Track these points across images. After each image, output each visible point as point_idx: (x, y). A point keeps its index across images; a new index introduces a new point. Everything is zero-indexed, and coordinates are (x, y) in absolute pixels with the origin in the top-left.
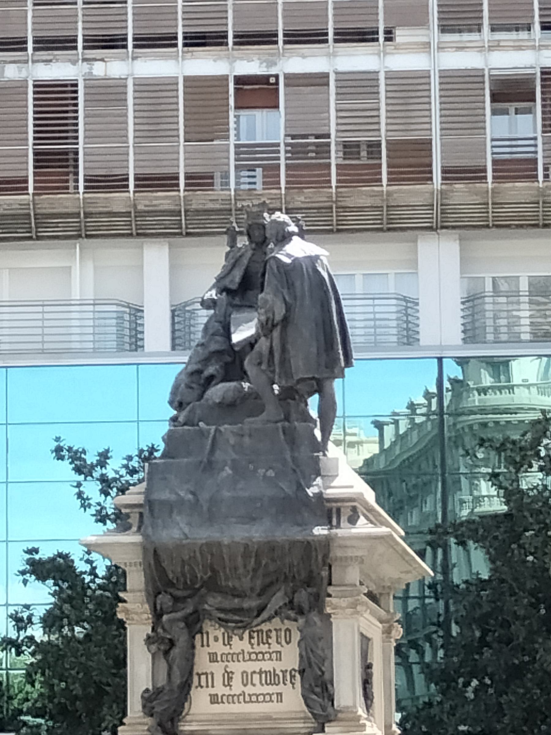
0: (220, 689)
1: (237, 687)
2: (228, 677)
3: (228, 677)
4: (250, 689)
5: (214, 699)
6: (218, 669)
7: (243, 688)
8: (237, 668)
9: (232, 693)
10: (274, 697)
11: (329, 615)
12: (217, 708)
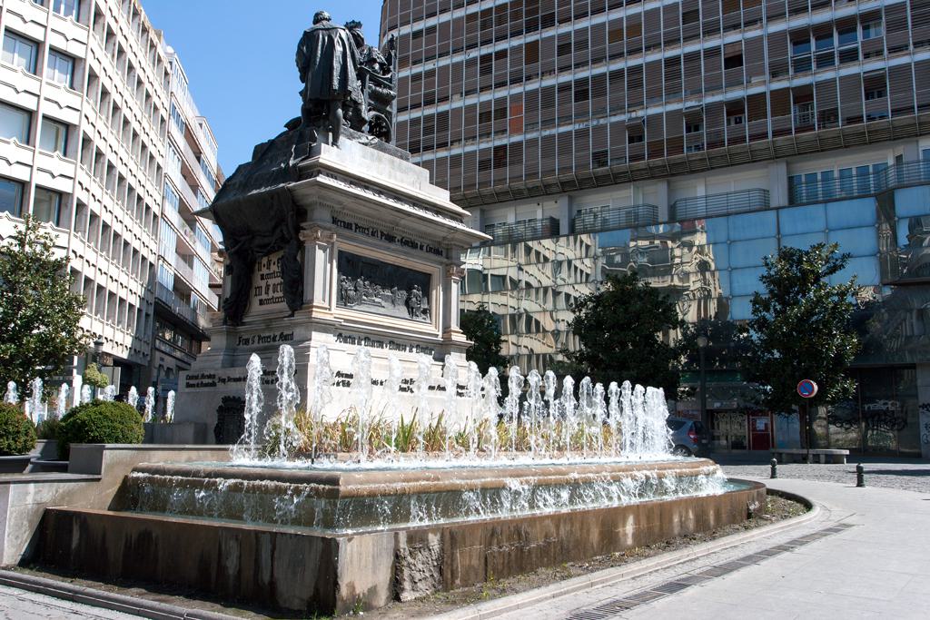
0: (264, 297)
1: (271, 294)
3: (268, 286)
5: (261, 302)
6: (263, 283)
8: (271, 282)
11: (303, 242)
12: (266, 307)
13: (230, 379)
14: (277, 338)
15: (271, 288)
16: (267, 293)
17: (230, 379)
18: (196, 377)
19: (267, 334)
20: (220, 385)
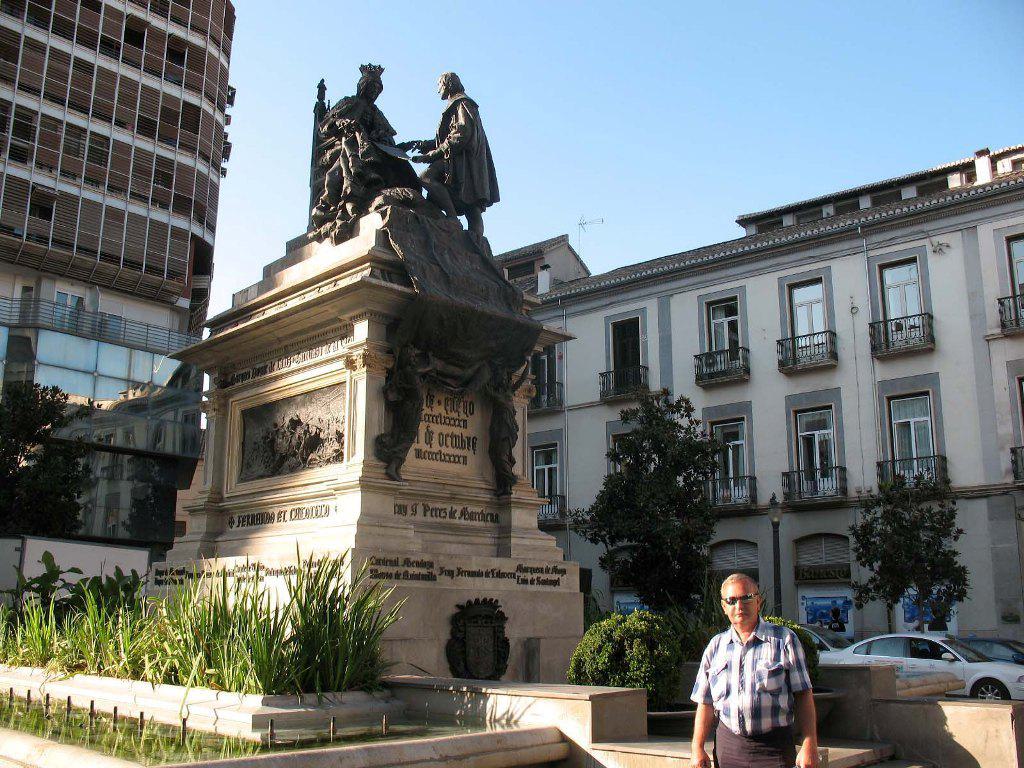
0: (425, 447)
2: (429, 434)
4: (444, 450)
5: (419, 454)
7: (440, 448)
8: (436, 428)
9: (433, 450)
10: (461, 459)
13: (460, 572)
14: (457, 515)
15: (435, 437)
16: (429, 442)
17: (460, 572)
18: (395, 563)
19: (439, 505)
20: (444, 581)
